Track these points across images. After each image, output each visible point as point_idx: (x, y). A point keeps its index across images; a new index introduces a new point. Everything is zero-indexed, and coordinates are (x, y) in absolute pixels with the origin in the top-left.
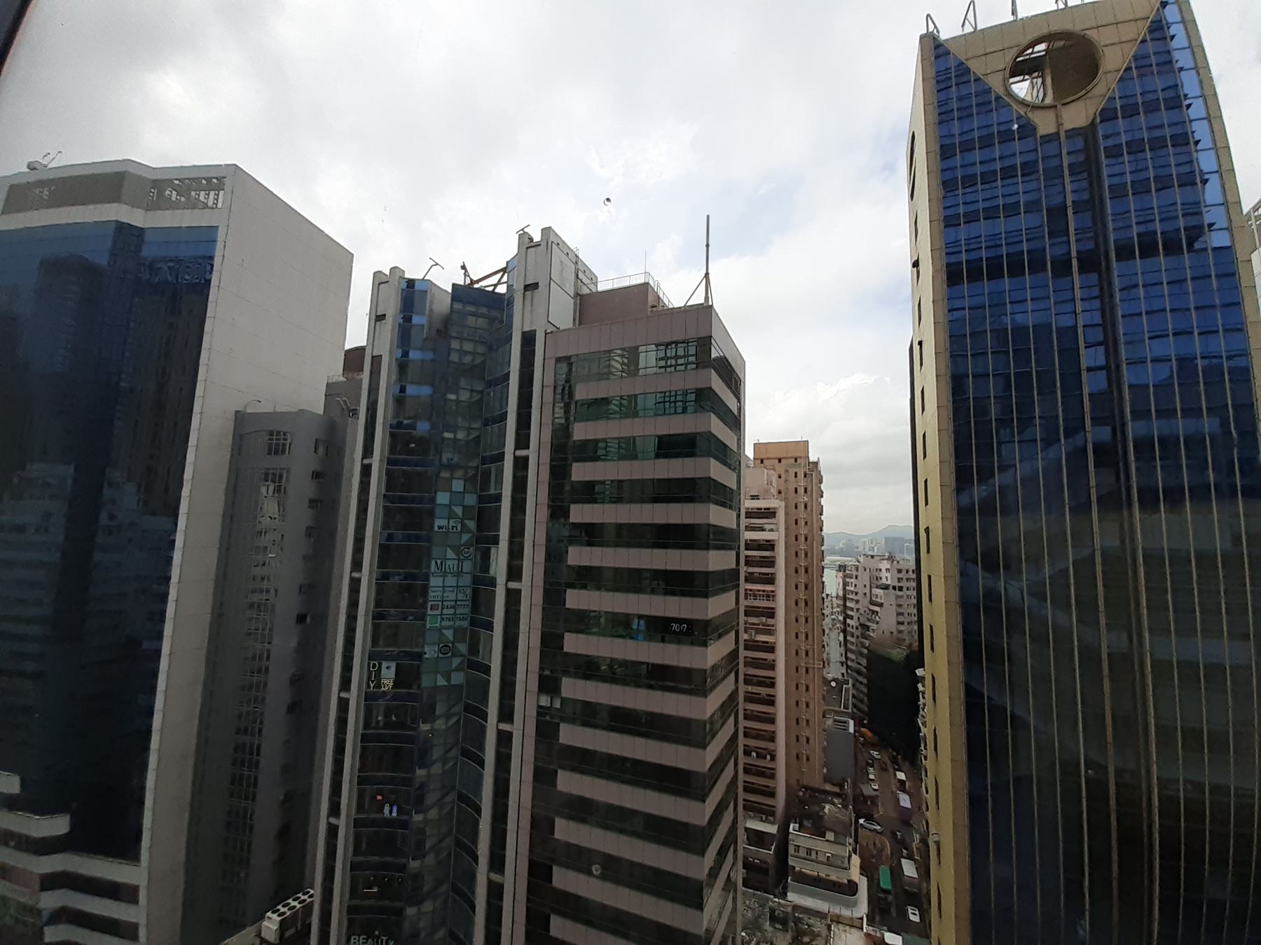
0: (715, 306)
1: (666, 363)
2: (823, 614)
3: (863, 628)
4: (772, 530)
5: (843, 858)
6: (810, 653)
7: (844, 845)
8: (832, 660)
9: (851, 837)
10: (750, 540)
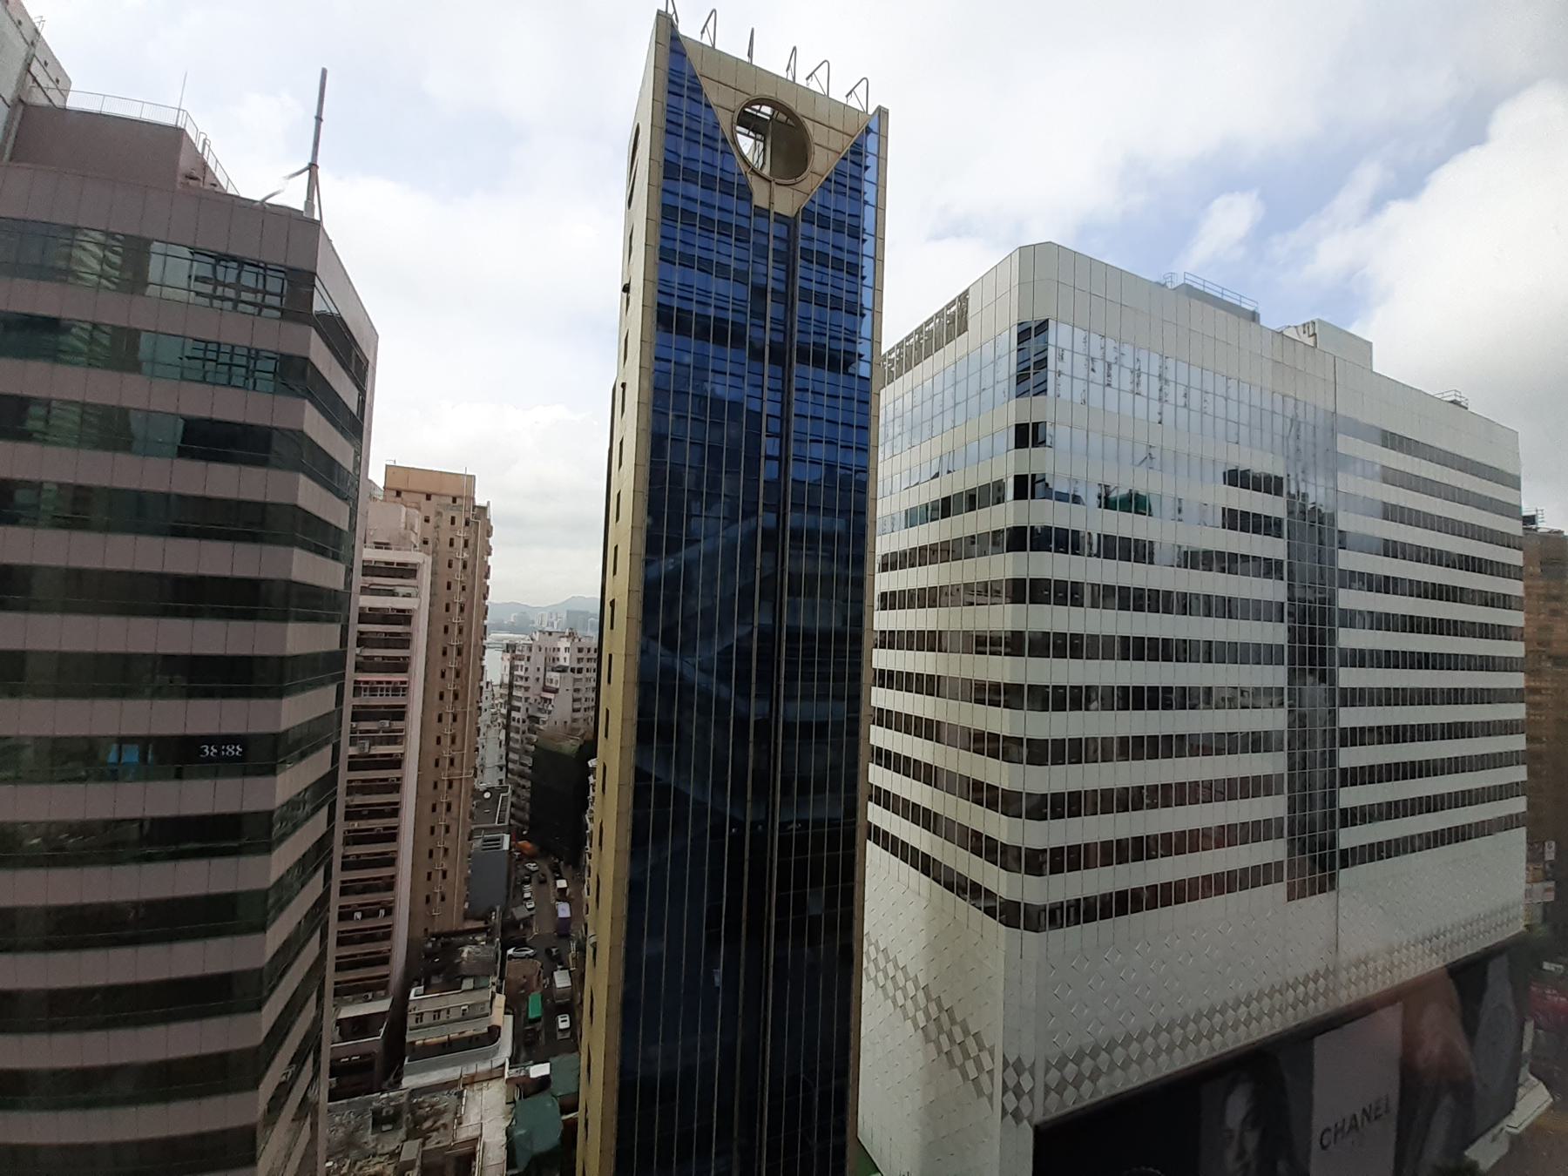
0: (326, 225)
1: (215, 290)
2: (480, 708)
4: (409, 595)
5: (483, 1003)
10: (370, 609)
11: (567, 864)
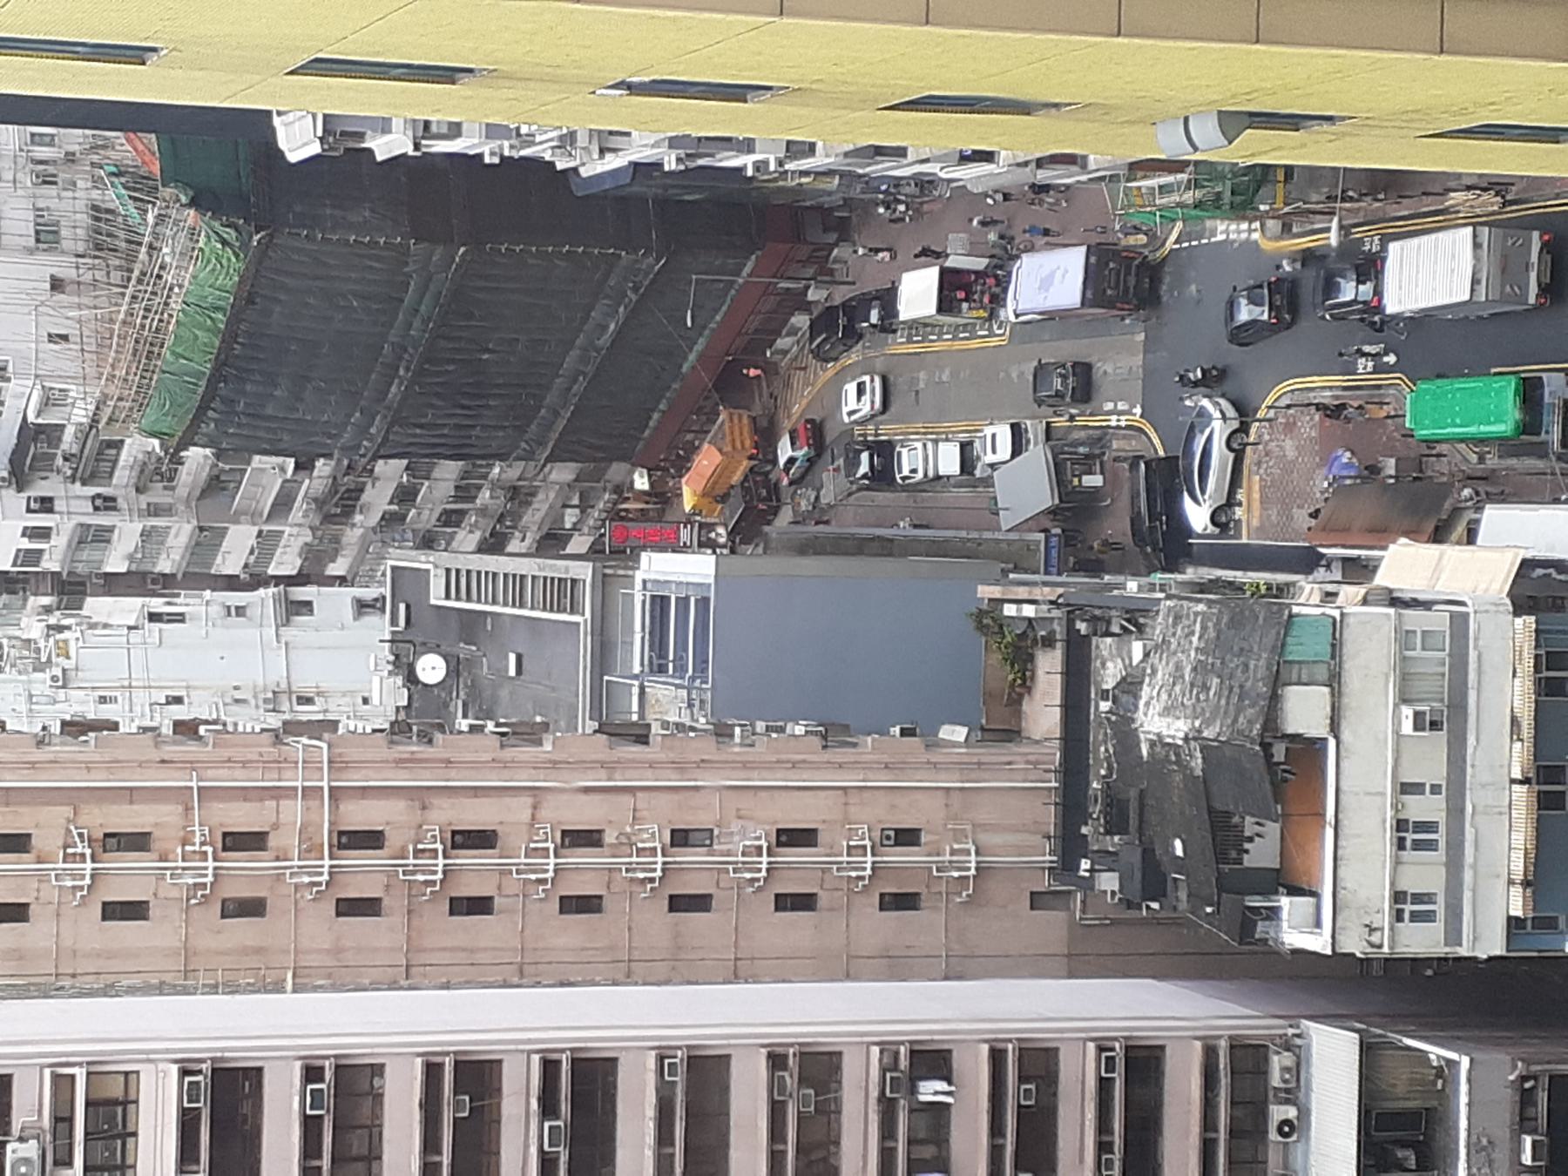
3: (44, 464)
5: (1404, 638)
6: (242, 818)
7: (1336, 628)
8: (277, 675)
9: (1282, 590)
11: (825, 274)
